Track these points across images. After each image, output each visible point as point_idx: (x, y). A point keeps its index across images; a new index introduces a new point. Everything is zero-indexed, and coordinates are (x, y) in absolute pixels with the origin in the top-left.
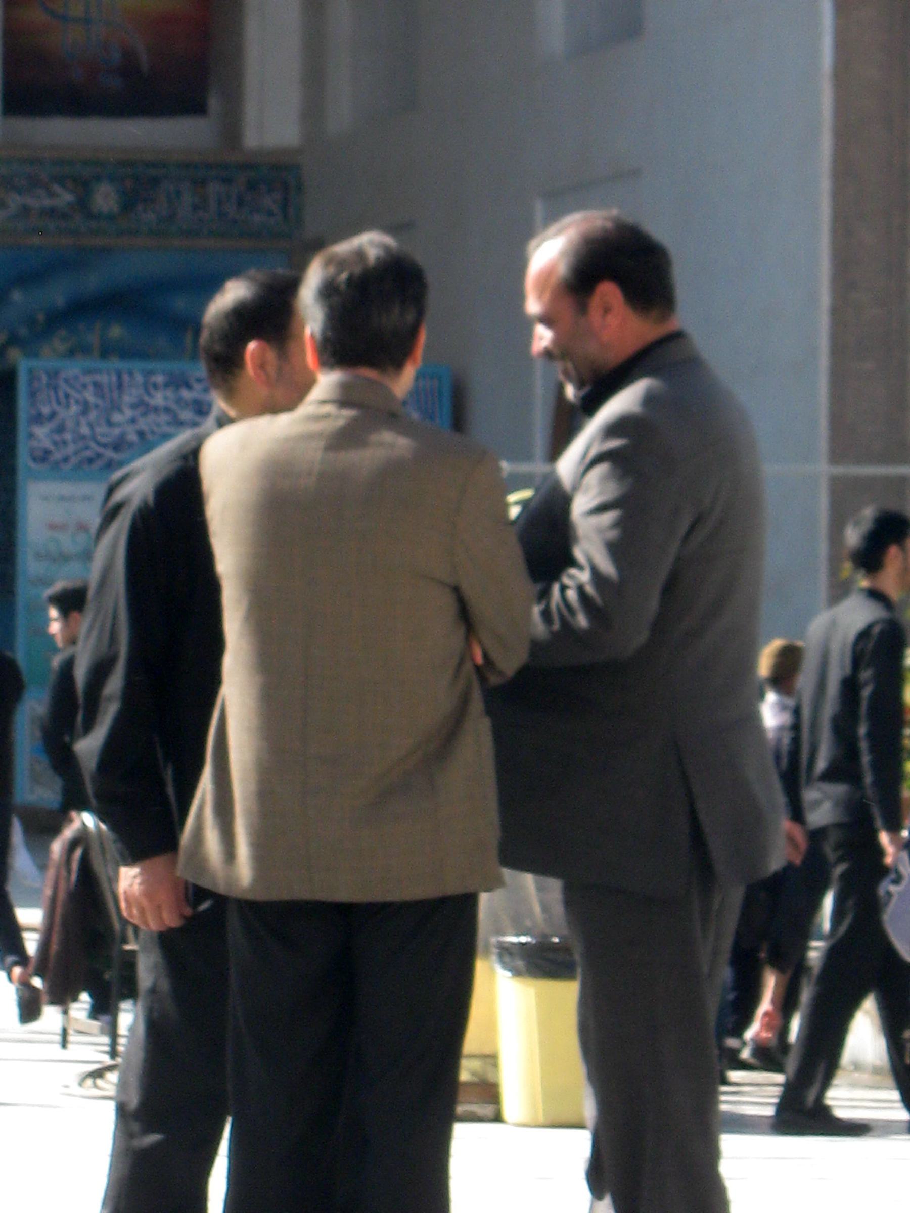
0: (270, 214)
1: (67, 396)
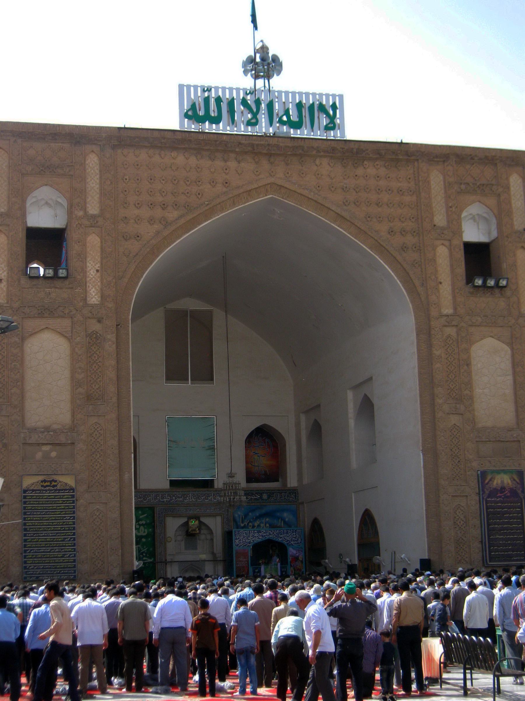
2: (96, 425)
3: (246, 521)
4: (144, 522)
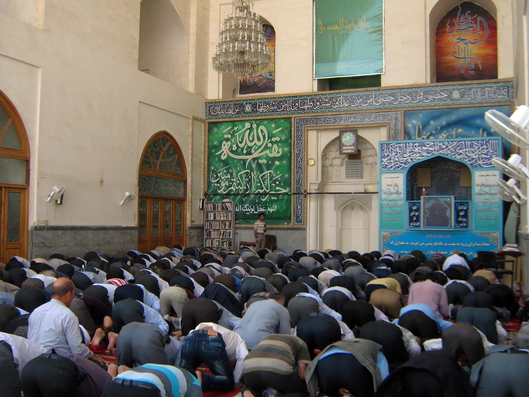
0: (504, 95)
1: (392, 150)
3: (425, 133)
4: (278, 139)
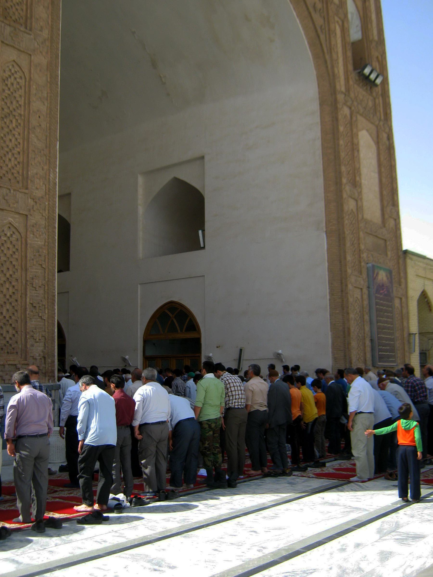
2: (13, 66)
